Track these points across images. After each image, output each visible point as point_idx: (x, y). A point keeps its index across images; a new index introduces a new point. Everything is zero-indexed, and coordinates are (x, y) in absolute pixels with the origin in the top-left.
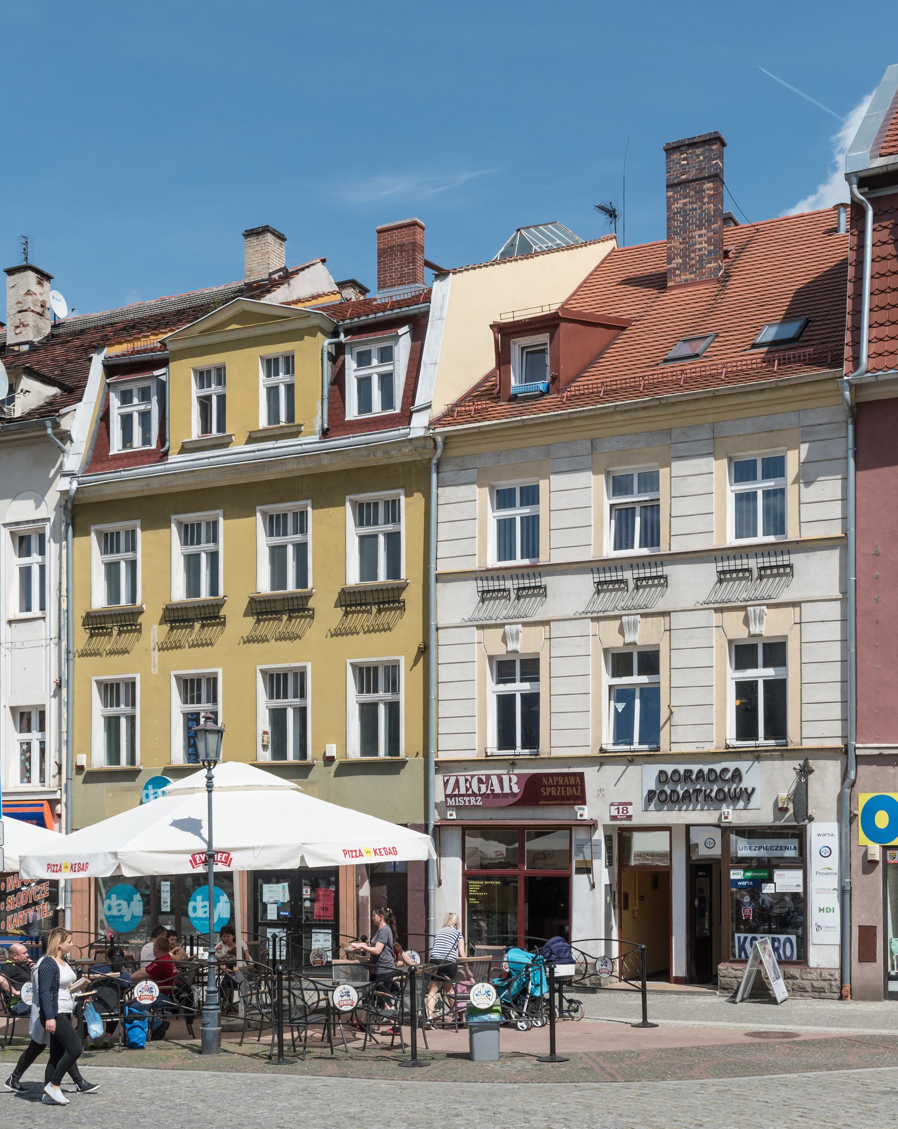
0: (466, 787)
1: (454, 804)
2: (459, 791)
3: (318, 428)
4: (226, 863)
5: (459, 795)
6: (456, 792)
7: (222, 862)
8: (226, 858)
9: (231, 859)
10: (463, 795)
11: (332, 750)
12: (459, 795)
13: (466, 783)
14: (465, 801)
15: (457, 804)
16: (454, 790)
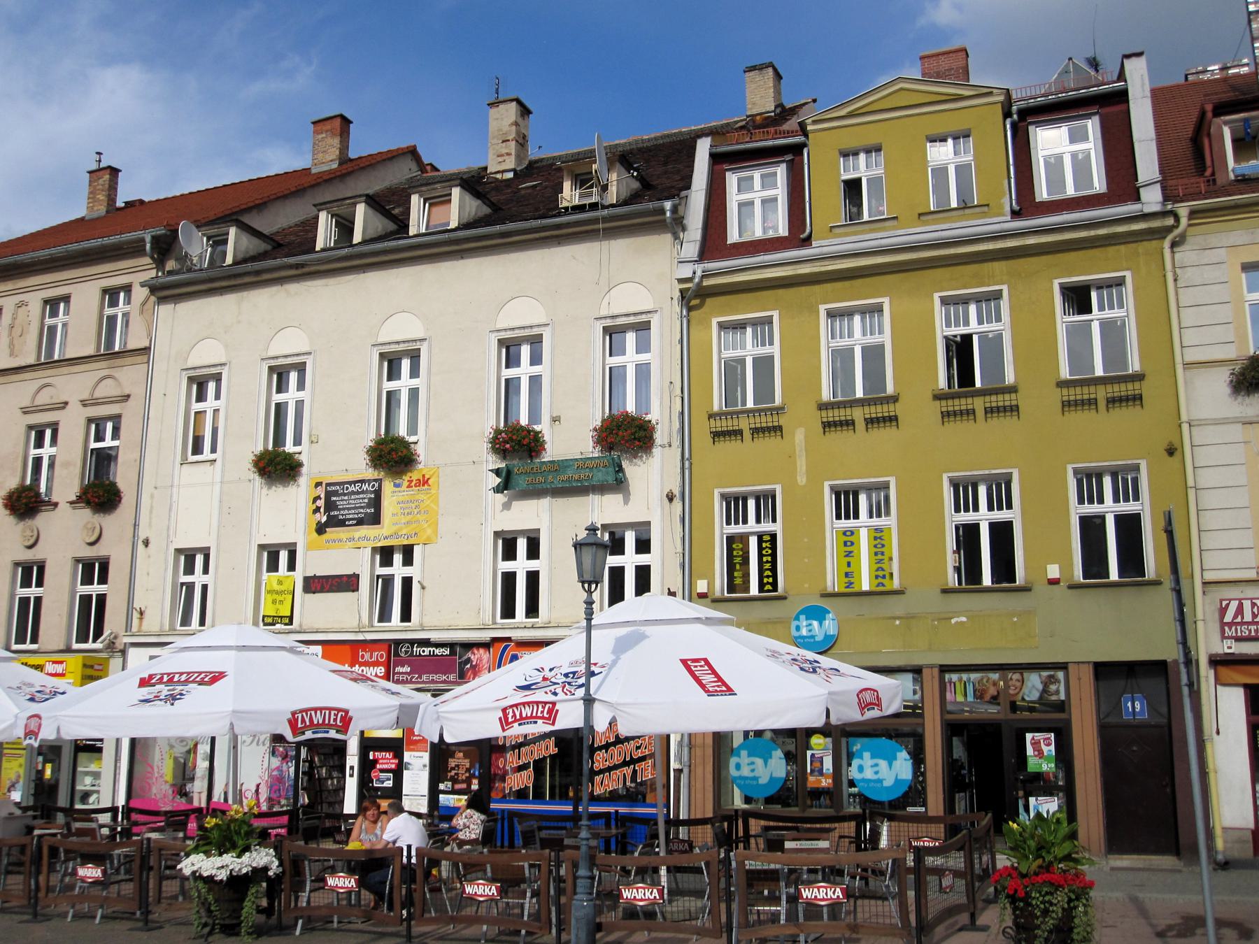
0: (1253, 613)
1: (1234, 634)
2: (1243, 618)
3: (1008, 209)
4: (549, 719)
5: (1242, 623)
6: (1239, 620)
7: (543, 718)
8: (550, 711)
9: (557, 711)
10: (1248, 623)
11: (1053, 571)
12: (1242, 623)
13: (1253, 608)
14: (1250, 631)
15: (1239, 634)
16: (1235, 617)
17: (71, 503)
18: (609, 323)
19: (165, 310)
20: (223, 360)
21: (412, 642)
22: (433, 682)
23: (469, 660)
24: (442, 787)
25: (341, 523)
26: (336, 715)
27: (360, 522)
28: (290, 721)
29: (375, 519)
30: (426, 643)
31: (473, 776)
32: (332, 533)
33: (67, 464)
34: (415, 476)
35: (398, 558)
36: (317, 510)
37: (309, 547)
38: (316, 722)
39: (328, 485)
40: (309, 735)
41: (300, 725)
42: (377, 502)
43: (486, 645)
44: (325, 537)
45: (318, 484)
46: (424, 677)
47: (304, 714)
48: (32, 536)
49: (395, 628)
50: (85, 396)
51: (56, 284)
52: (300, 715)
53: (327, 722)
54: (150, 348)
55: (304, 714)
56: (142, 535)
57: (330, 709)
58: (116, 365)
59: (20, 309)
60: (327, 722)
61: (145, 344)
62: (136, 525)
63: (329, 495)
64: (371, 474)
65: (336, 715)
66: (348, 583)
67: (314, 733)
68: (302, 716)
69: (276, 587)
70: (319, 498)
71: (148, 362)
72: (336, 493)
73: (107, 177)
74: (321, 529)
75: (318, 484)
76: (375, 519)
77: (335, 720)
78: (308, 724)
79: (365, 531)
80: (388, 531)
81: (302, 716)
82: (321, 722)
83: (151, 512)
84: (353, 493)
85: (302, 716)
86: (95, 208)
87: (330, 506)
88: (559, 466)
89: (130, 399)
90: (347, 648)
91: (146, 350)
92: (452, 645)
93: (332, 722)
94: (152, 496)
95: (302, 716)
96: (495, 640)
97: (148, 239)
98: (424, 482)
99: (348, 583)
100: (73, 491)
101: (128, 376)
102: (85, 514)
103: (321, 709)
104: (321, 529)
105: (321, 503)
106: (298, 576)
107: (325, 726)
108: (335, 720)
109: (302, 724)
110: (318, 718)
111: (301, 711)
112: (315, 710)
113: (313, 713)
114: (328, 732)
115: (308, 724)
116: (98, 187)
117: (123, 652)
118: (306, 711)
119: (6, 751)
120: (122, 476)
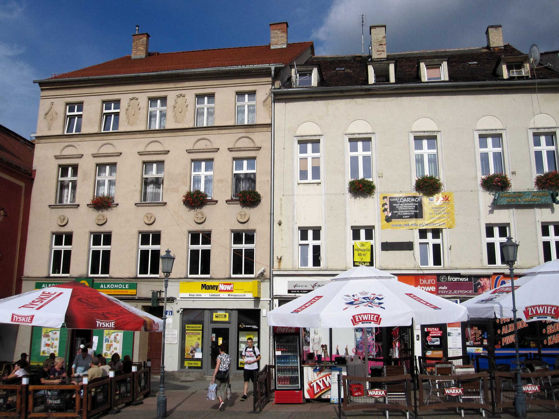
17: (227, 201)
18: (535, 131)
19: (279, 106)
20: (320, 133)
21: (447, 275)
22: (460, 294)
23: (479, 284)
24: (468, 343)
25: (401, 217)
26: (551, 309)
27: (411, 217)
28: (524, 312)
30: (458, 275)
31: (484, 338)
32: (395, 222)
33: (221, 181)
35: (430, 235)
36: (385, 210)
37: (383, 228)
38: (539, 312)
39: (390, 198)
40: (535, 319)
41: (530, 314)
43: (488, 277)
44: (391, 223)
45: (384, 198)
46: (455, 292)
47: (532, 308)
48: (202, 218)
49: (438, 270)
50: (231, 146)
51: (204, 87)
52: (530, 309)
53: (546, 312)
54: (271, 124)
55: (532, 308)
57: (547, 306)
58: (250, 131)
59: (178, 98)
60: (546, 312)
61: (269, 122)
62: (272, 214)
63: (391, 203)
64: (414, 193)
65: (551, 309)
66: (408, 246)
67: (538, 318)
68: (532, 310)
69: (360, 247)
70: (386, 204)
71: (271, 131)
72: (396, 202)
73: (145, 38)
74: (388, 220)
75: (384, 198)
77: (551, 311)
78: (535, 313)
79: (413, 221)
80: (425, 223)
81: (532, 310)
82: (542, 312)
83: (281, 207)
84: (406, 202)
85: (531, 309)
86: (138, 54)
87: (392, 208)
88: (519, 194)
89: (169, 153)
90: (413, 277)
91: (269, 125)
92: (470, 277)
93: (549, 312)
94: (281, 200)
95: (531, 309)
96: (495, 274)
97: (273, 68)
99: (408, 246)
102: (237, 208)
103: (542, 306)
105: (387, 207)
106: (377, 242)
107: (544, 315)
108: (551, 311)
109: (531, 313)
110: (540, 311)
111: (531, 307)
112: (539, 306)
113: (537, 308)
114: (546, 318)
115: (535, 313)
116: (139, 43)
117: (270, 280)
118: (534, 307)
119: (187, 331)
120: (261, 188)
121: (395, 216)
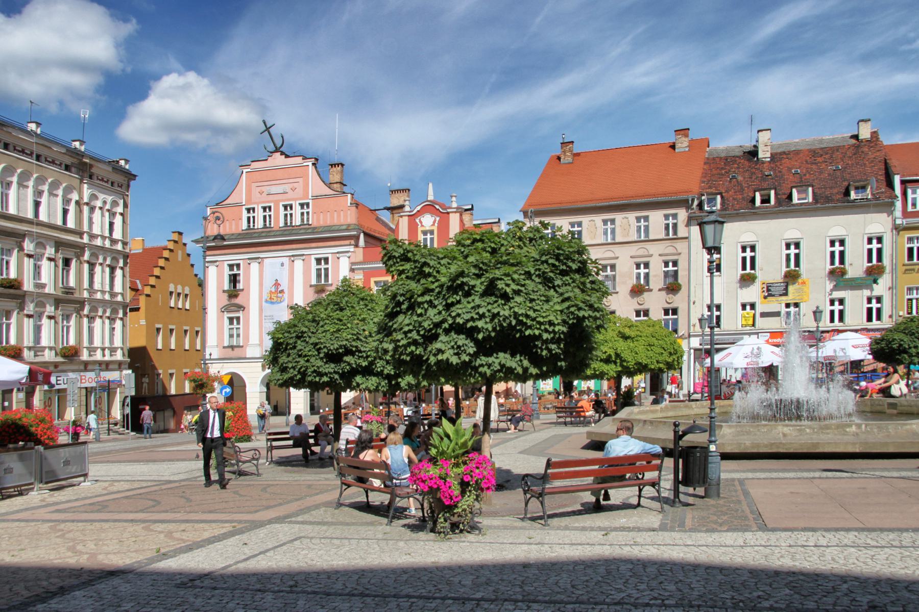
25: (773, 296)
27: (781, 295)
29: (786, 294)
32: (770, 299)
33: (655, 276)
34: (800, 280)
42: (786, 289)
50: (661, 253)
56: (692, 300)
61: (686, 235)
62: (689, 296)
63: (768, 287)
66: (777, 314)
74: (765, 297)
76: (786, 294)
79: (784, 298)
80: (790, 299)
87: (768, 290)
98: (804, 283)
99: (777, 314)
100: (661, 285)
101: (681, 246)
104: (765, 297)
105: (765, 289)
120: (682, 280)
121: (770, 295)
